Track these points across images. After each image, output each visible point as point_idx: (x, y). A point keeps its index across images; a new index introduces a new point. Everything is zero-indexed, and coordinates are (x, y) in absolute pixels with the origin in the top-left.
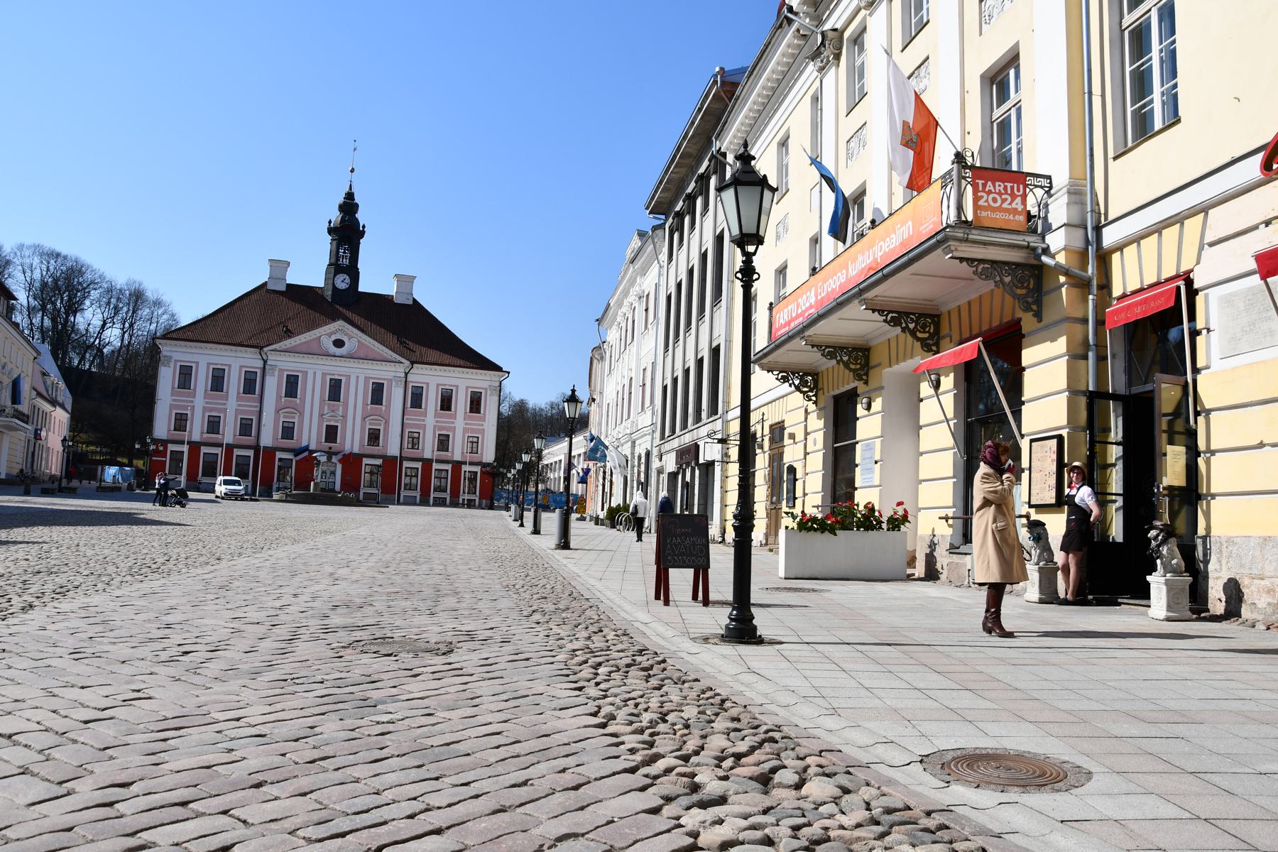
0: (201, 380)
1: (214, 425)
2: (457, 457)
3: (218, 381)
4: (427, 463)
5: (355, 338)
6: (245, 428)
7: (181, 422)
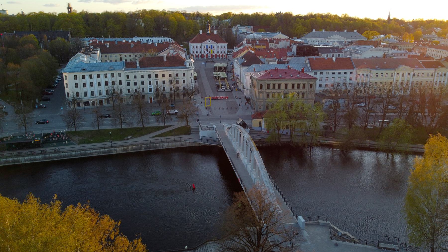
0: (195, 47)
1: (197, 52)
2: (223, 53)
3: (197, 47)
4: (220, 54)
5: (211, 41)
6: (200, 52)
7: (194, 52)
